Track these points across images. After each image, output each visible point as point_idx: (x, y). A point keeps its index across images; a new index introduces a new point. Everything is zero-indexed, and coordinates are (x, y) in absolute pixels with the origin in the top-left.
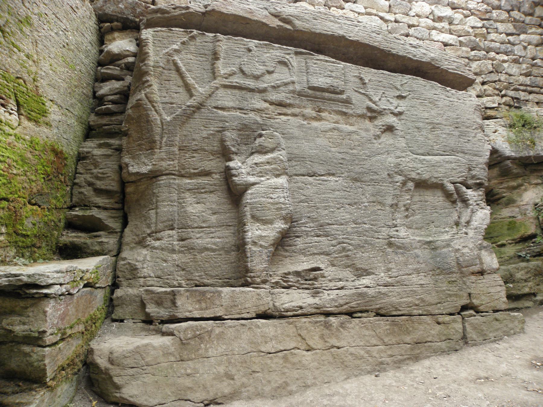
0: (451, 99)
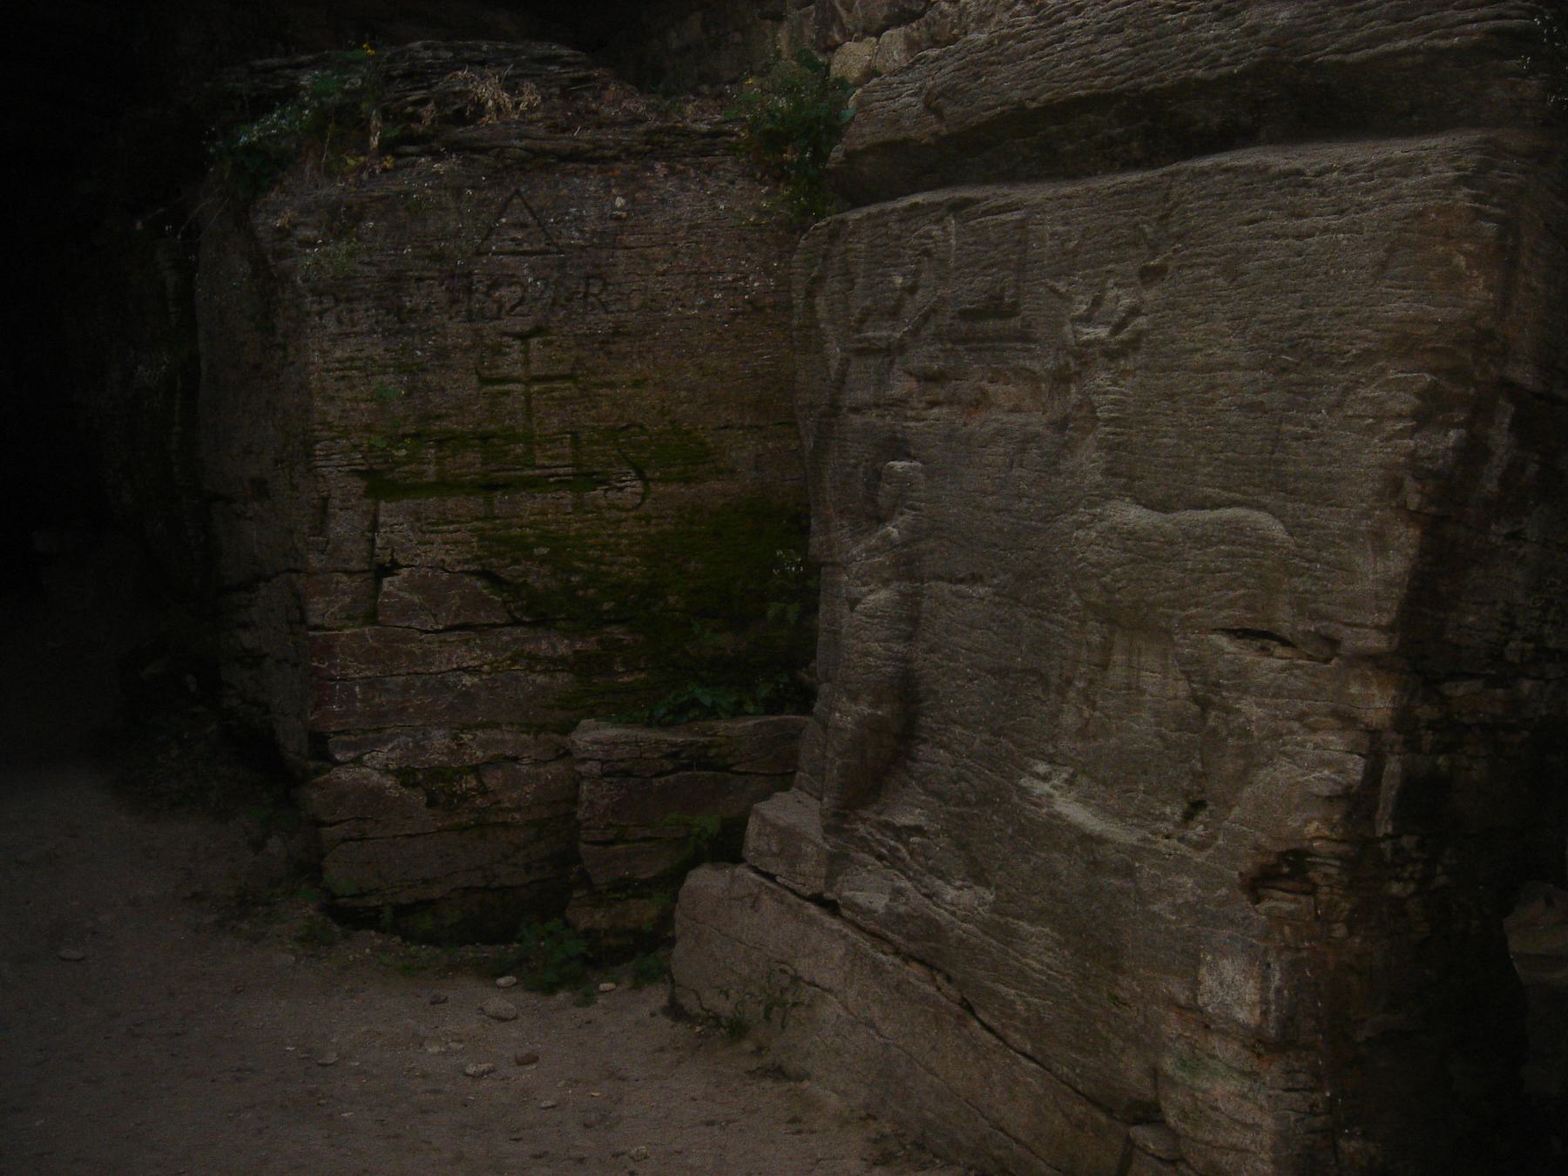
0: (1306, 224)
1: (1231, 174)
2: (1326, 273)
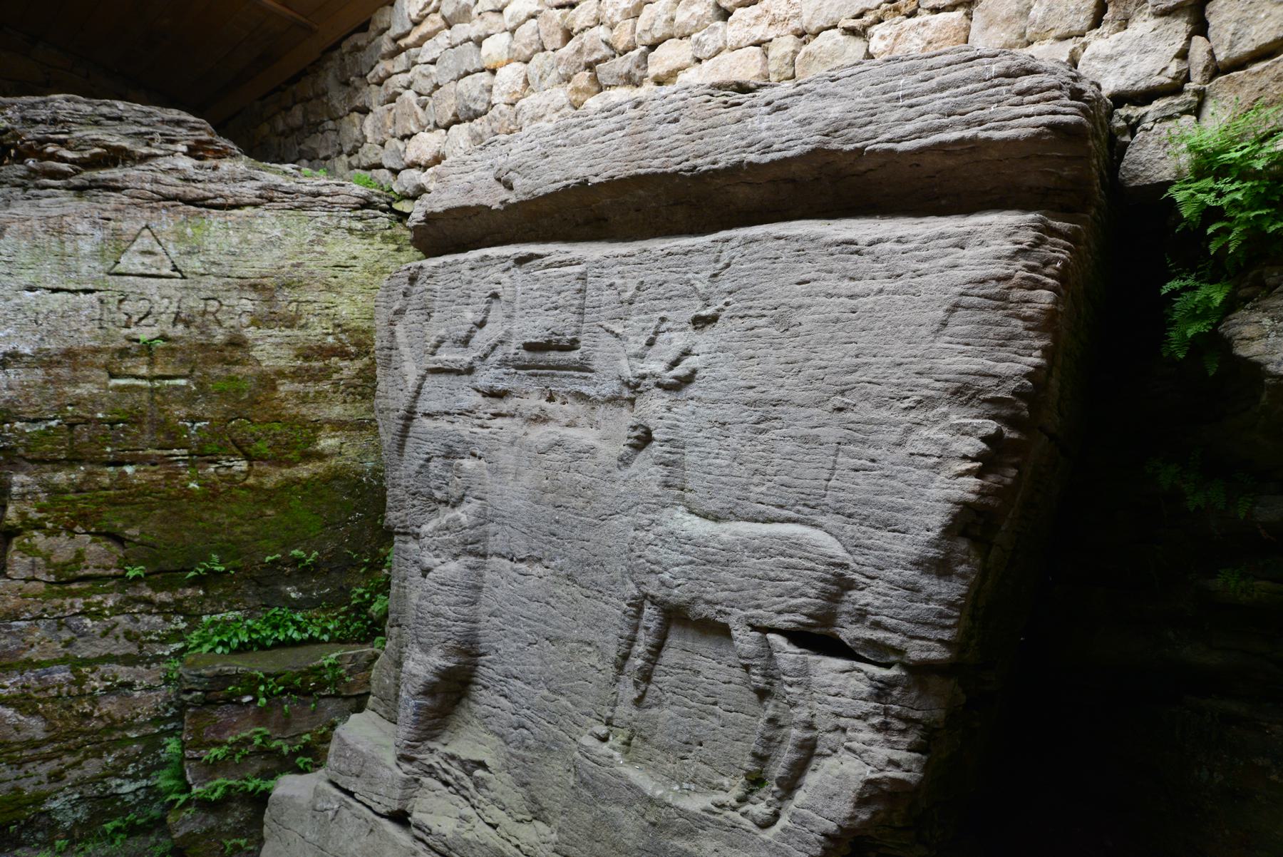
0: (859, 286)
1: (782, 242)
2: (884, 327)
